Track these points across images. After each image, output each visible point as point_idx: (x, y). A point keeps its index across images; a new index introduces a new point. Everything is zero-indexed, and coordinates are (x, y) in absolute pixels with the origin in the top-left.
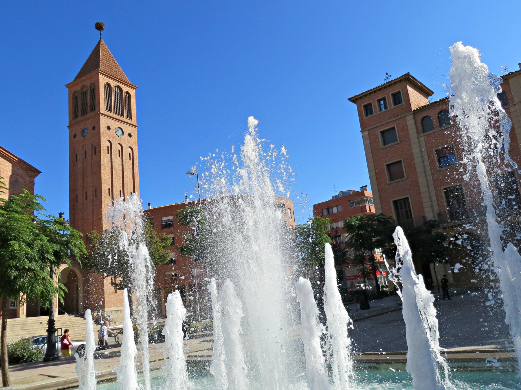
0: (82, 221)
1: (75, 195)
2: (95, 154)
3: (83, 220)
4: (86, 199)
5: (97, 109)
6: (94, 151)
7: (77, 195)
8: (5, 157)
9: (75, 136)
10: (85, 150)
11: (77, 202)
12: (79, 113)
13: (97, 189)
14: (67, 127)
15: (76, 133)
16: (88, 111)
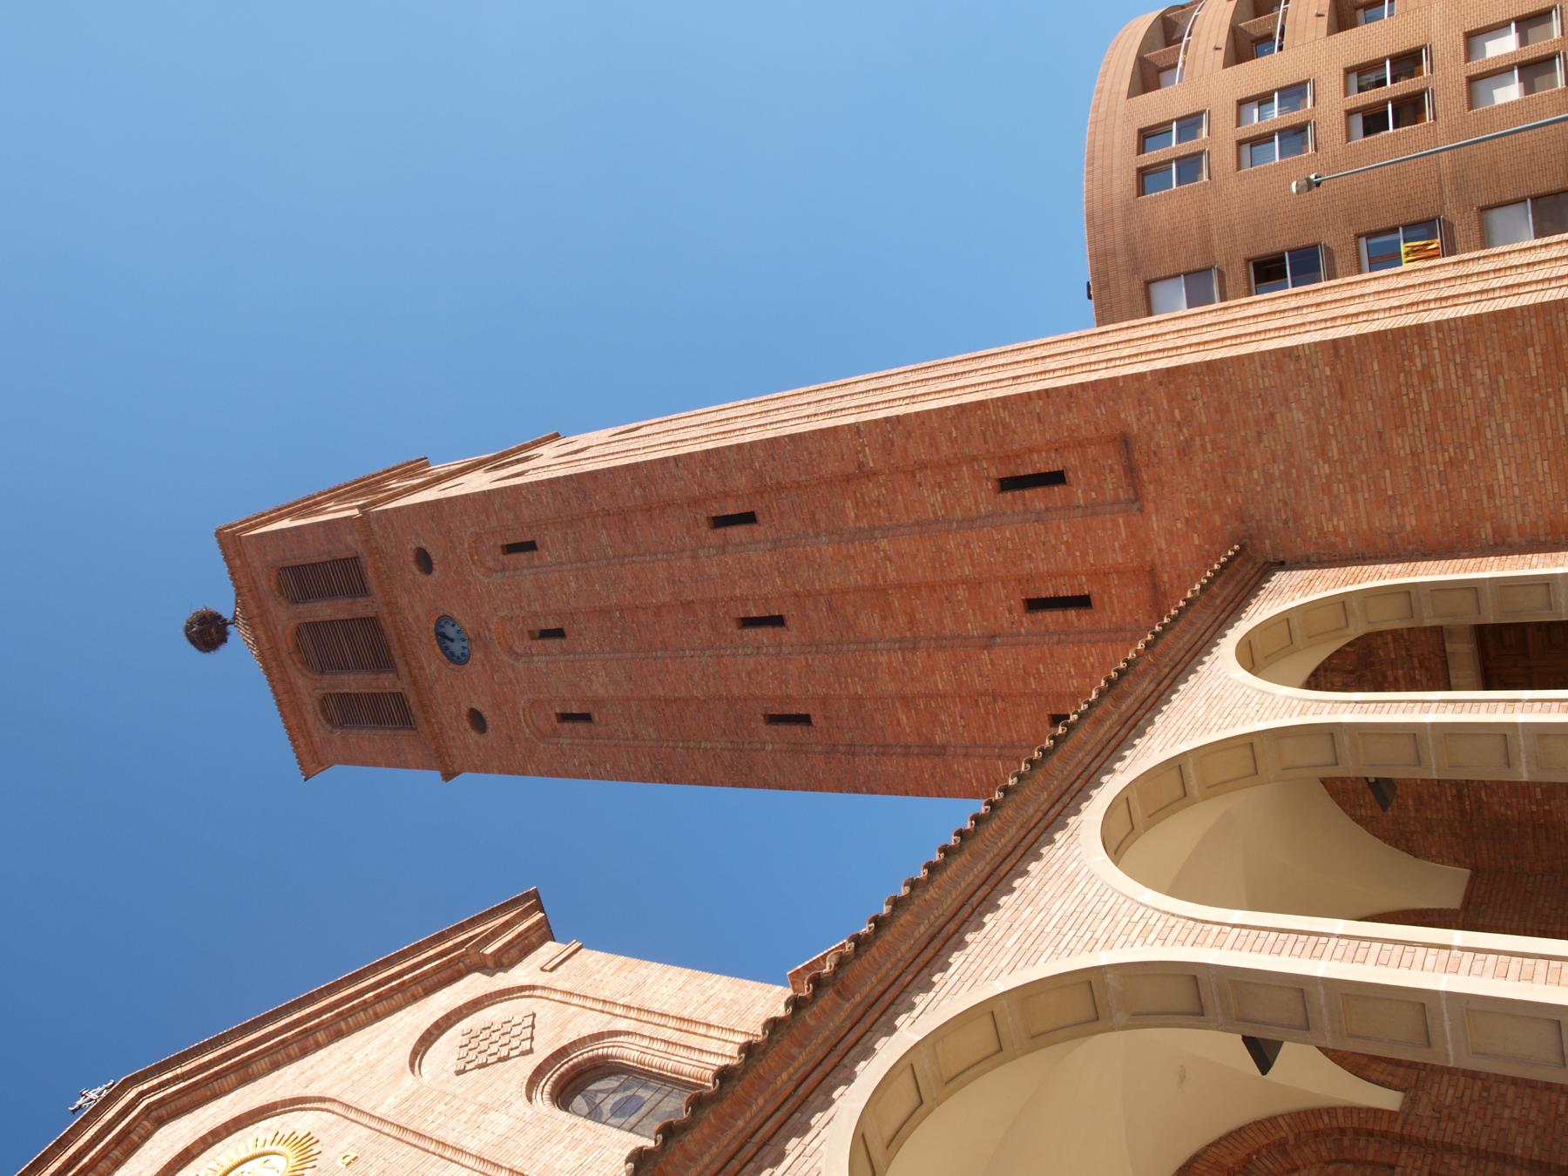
0: (920, 659)
1: (765, 730)
2: (530, 546)
3: (915, 649)
4: (777, 621)
5: (352, 543)
6: (523, 557)
7: (773, 719)
8: (294, 1049)
9: (477, 721)
10: (527, 642)
11: (805, 719)
12: (386, 682)
13: (717, 509)
14: (448, 776)
15: (464, 710)
16: (370, 613)
